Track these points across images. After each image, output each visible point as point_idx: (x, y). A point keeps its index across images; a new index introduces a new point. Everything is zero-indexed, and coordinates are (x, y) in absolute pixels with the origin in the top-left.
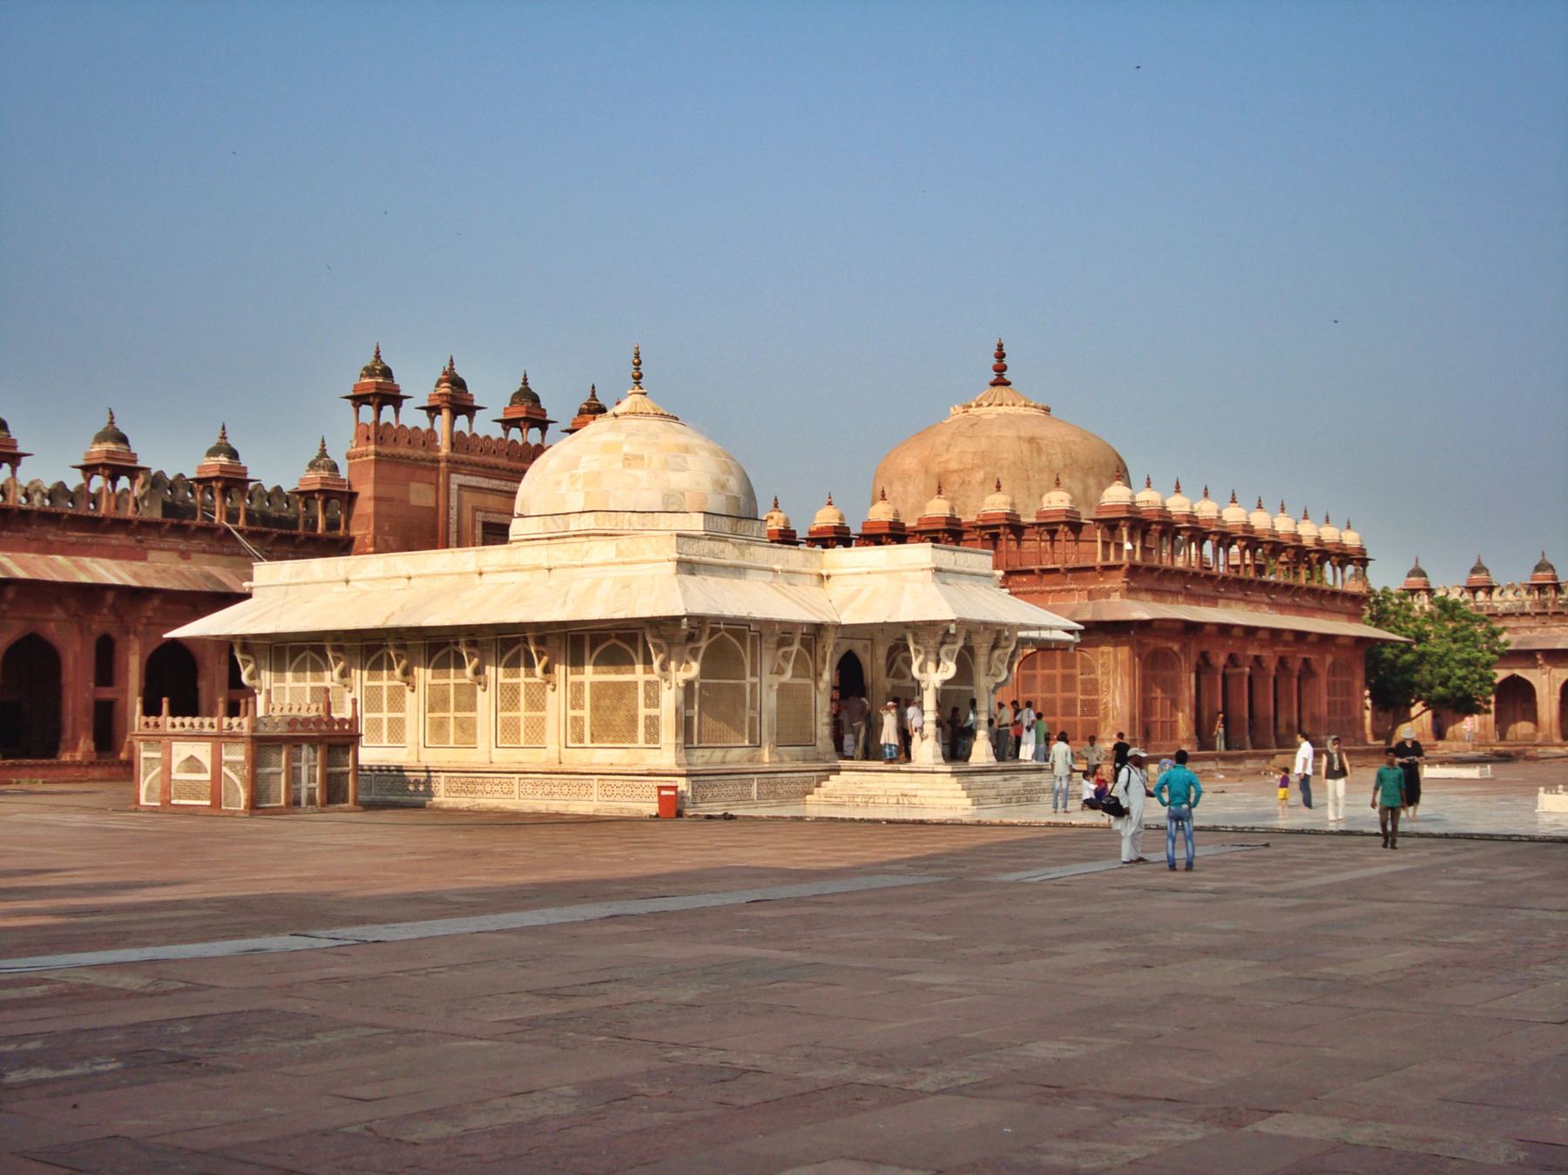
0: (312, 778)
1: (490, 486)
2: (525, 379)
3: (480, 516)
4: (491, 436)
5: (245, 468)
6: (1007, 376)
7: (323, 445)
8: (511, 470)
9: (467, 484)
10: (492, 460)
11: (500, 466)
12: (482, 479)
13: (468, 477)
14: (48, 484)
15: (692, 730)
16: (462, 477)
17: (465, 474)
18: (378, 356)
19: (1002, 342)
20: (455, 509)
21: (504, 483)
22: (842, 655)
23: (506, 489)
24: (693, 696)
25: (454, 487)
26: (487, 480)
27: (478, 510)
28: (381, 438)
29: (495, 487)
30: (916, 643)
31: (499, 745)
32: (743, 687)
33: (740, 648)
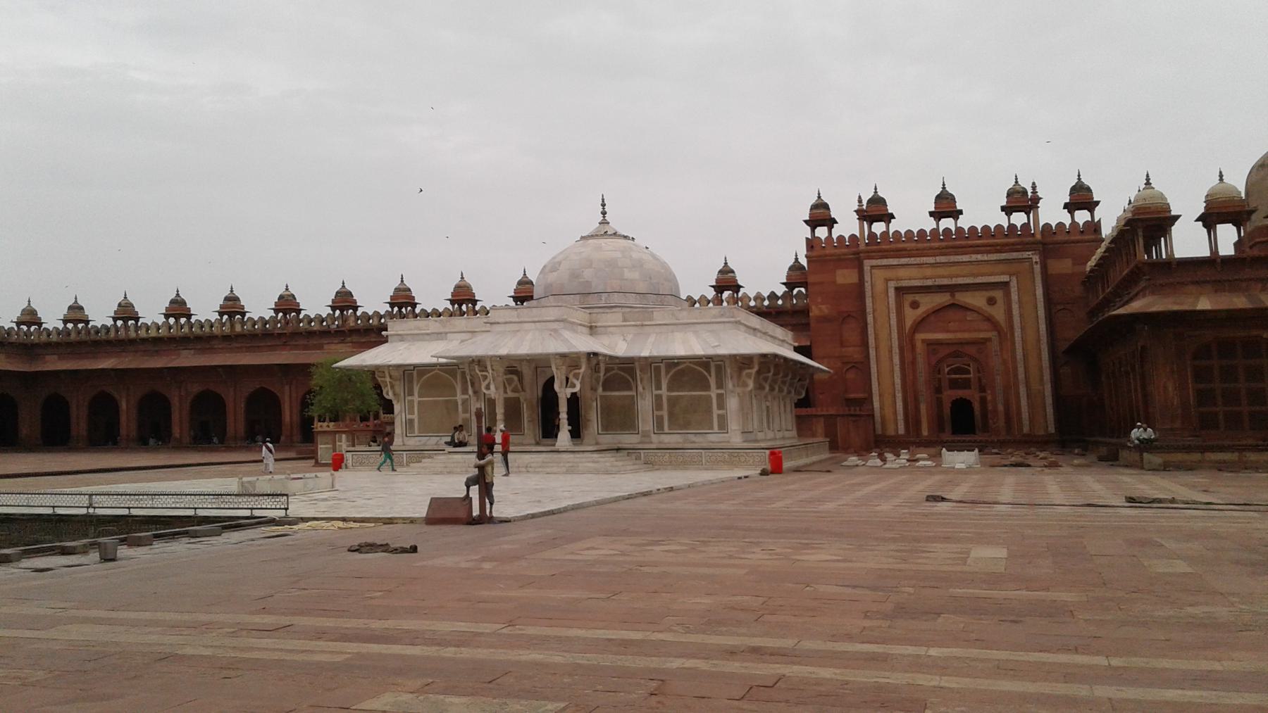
1: (900, 263)
3: (892, 285)
4: (900, 230)
7: (796, 256)
9: (879, 264)
11: (908, 249)
12: (891, 260)
13: (879, 260)
14: (766, 294)
15: (414, 427)
16: (874, 261)
20: (870, 282)
21: (912, 259)
22: (546, 379)
23: (915, 262)
24: (413, 407)
25: (867, 268)
26: (898, 259)
27: (890, 280)
28: (812, 247)
29: (905, 263)
30: (493, 370)
31: (637, 432)
32: (456, 402)
33: (452, 379)
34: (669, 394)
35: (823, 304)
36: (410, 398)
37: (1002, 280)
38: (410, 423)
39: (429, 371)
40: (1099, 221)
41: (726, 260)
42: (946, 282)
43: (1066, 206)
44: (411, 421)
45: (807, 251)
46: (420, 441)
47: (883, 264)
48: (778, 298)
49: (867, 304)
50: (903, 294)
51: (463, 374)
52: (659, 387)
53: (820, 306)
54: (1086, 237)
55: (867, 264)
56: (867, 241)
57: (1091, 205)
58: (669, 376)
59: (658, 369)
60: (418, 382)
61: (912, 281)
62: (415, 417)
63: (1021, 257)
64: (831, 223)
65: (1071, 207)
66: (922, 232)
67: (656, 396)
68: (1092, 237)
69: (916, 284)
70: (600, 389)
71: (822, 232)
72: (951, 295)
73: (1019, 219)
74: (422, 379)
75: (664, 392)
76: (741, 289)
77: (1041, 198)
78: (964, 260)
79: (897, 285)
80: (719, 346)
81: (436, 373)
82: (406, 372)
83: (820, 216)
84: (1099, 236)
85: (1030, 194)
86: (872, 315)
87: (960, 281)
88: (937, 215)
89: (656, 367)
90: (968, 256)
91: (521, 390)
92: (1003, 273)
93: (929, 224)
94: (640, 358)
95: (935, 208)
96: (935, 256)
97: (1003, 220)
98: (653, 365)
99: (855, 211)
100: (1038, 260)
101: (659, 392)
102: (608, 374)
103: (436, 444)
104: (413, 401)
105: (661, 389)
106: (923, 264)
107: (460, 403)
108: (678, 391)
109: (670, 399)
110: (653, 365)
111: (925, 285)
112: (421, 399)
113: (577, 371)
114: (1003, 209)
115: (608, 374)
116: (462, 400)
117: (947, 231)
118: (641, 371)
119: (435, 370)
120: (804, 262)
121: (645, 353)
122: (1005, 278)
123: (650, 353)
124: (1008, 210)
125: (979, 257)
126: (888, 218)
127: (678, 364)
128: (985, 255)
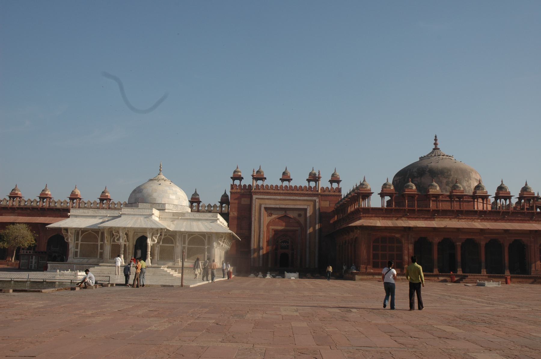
0: (35, 263)
1: (267, 198)
2: (286, 168)
5: (510, 192)
6: (438, 147)
7: (225, 191)
8: (275, 193)
10: (267, 191)
11: (271, 192)
12: (264, 196)
13: (259, 196)
14: (207, 205)
16: (257, 196)
17: (258, 195)
18: (237, 168)
19: (437, 135)
20: (254, 204)
21: (272, 196)
22: (138, 237)
23: (273, 198)
26: (266, 196)
32: (97, 245)
33: (96, 235)
34: (188, 246)
35: (235, 212)
36: (77, 242)
37: (305, 208)
38: (76, 252)
39: (87, 231)
40: (341, 188)
41: (196, 190)
42: (283, 206)
43: (330, 181)
44: (76, 252)
45: (231, 190)
46: (80, 260)
47: (260, 197)
48: (211, 207)
49: (253, 213)
50: (267, 210)
51: (103, 234)
52: (184, 243)
53: (234, 212)
54: (336, 194)
55: (254, 197)
56: (255, 188)
57: (338, 182)
58: (189, 239)
59: (185, 236)
60: (81, 235)
61: (271, 205)
62: (79, 250)
63: (312, 199)
64: (240, 178)
65: (331, 182)
66: (277, 186)
67: (183, 247)
68: (338, 194)
69: (272, 207)
70: (161, 243)
71: (237, 182)
72: (285, 212)
73: (313, 184)
74: (83, 234)
75: (186, 245)
76: (201, 203)
77: (321, 177)
78: (291, 198)
79: (265, 207)
80: (211, 229)
81: (90, 232)
82: (76, 231)
83: (237, 177)
84: (340, 194)
85: (317, 176)
86: (254, 218)
87: (289, 207)
88: (282, 180)
89: (184, 235)
90: (293, 197)
91: (127, 241)
92: (305, 205)
93: (279, 183)
94: (180, 232)
95: (282, 177)
96: (280, 196)
97: (306, 184)
98: (183, 234)
99: (251, 175)
100: (318, 201)
101: (184, 245)
102: (165, 237)
103: (87, 262)
104: (78, 243)
105: (185, 244)
106: (276, 199)
107: (99, 245)
108: (192, 245)
109: (188, 248)
110: (183, 235)
111: (276, 207)
112: (81, 243)
113: (156, 235)
114: (307, 180)
115: (165, 237)
116: (100, 244)
117: (286, 186)
118: (179, 236)
119: (89, 231)
120: (229, 194)
121: (183, 230)
122: (305, 207)
123: (185, 229)
124: (309, 181)
125: (297, 198)
126: (263, 179)
127: (192, 235)
128: (299, 197)
